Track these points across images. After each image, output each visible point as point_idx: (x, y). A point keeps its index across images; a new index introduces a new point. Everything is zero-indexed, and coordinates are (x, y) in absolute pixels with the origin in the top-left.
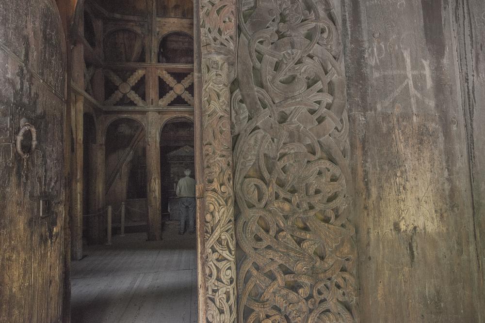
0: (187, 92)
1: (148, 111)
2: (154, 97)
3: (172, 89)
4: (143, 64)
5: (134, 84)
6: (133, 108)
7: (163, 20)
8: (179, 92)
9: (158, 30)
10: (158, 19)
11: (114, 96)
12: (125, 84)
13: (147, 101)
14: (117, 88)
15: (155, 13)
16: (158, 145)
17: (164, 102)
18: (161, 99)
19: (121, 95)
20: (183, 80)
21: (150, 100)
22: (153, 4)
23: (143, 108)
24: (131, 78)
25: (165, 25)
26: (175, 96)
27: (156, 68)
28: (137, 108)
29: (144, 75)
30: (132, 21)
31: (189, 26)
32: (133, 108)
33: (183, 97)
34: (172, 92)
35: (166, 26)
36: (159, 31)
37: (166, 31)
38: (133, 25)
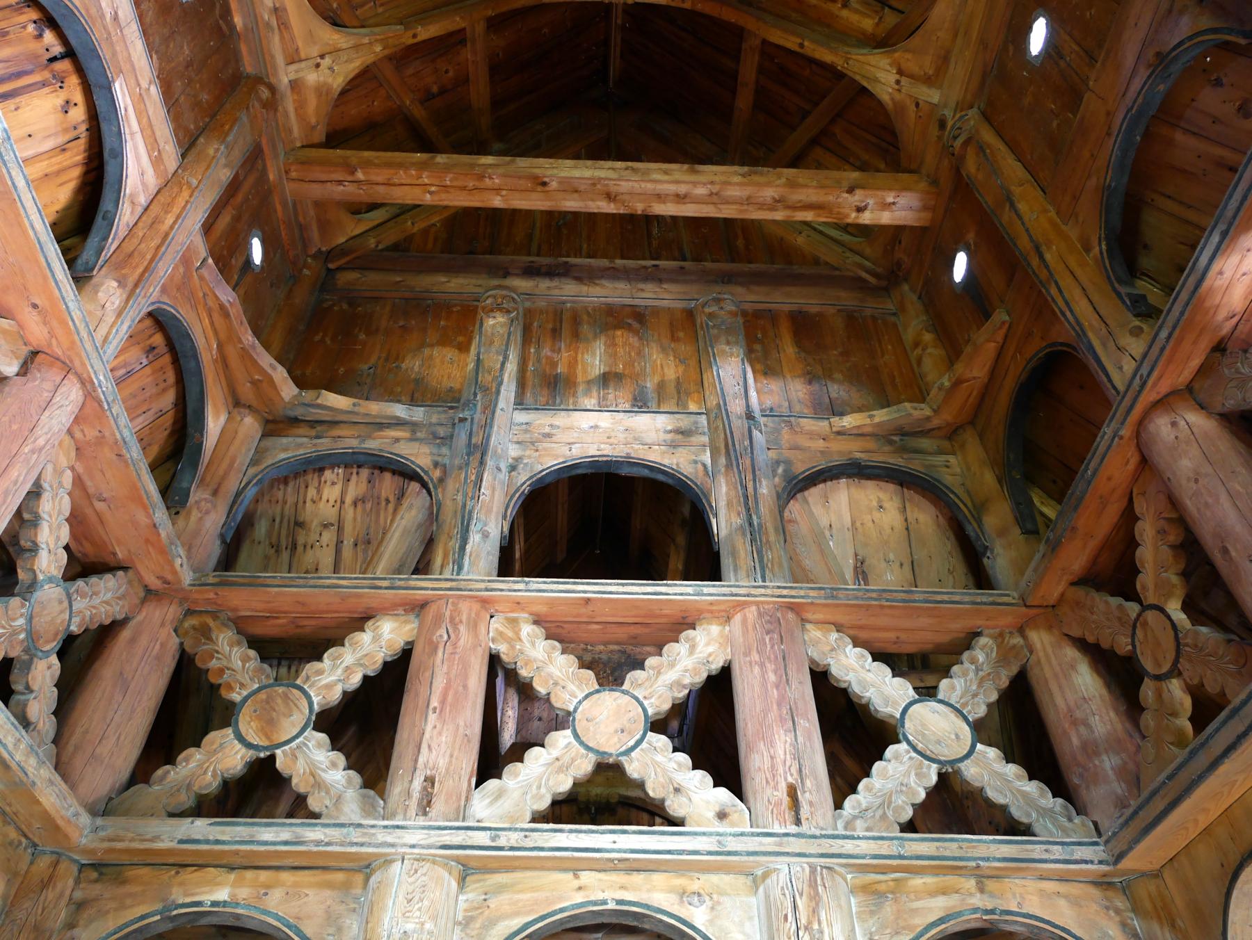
0: (661, 741)
1: (388, 862)
2: (442, 763)
3: (561, 721)
4: (418, 581)
5: (335, 696)
6: (285, 835)
7: (542, 421)
8: (612, 746)
9: (513, 451)
10: (521, 417)
12: (281, 690)
13: (396, 789)
14: (225, 714)
15: (508, 391)
17: (506, 805)
18: (492, 784)
20: (637, 674)
21: (418, 784)
22: (503, 364)
23: (355, 835)
25: (549, 435)
26: (585, 766)
27: (485, 602)
28: (313, 834)
29: (406, 654)
30: (399, 423)
31: (669, 437)
32: (285, 835)
33: (633, 769)
35: (554, 439)
36: (518, 460)
37: (557, 457)
38: (397, 440)
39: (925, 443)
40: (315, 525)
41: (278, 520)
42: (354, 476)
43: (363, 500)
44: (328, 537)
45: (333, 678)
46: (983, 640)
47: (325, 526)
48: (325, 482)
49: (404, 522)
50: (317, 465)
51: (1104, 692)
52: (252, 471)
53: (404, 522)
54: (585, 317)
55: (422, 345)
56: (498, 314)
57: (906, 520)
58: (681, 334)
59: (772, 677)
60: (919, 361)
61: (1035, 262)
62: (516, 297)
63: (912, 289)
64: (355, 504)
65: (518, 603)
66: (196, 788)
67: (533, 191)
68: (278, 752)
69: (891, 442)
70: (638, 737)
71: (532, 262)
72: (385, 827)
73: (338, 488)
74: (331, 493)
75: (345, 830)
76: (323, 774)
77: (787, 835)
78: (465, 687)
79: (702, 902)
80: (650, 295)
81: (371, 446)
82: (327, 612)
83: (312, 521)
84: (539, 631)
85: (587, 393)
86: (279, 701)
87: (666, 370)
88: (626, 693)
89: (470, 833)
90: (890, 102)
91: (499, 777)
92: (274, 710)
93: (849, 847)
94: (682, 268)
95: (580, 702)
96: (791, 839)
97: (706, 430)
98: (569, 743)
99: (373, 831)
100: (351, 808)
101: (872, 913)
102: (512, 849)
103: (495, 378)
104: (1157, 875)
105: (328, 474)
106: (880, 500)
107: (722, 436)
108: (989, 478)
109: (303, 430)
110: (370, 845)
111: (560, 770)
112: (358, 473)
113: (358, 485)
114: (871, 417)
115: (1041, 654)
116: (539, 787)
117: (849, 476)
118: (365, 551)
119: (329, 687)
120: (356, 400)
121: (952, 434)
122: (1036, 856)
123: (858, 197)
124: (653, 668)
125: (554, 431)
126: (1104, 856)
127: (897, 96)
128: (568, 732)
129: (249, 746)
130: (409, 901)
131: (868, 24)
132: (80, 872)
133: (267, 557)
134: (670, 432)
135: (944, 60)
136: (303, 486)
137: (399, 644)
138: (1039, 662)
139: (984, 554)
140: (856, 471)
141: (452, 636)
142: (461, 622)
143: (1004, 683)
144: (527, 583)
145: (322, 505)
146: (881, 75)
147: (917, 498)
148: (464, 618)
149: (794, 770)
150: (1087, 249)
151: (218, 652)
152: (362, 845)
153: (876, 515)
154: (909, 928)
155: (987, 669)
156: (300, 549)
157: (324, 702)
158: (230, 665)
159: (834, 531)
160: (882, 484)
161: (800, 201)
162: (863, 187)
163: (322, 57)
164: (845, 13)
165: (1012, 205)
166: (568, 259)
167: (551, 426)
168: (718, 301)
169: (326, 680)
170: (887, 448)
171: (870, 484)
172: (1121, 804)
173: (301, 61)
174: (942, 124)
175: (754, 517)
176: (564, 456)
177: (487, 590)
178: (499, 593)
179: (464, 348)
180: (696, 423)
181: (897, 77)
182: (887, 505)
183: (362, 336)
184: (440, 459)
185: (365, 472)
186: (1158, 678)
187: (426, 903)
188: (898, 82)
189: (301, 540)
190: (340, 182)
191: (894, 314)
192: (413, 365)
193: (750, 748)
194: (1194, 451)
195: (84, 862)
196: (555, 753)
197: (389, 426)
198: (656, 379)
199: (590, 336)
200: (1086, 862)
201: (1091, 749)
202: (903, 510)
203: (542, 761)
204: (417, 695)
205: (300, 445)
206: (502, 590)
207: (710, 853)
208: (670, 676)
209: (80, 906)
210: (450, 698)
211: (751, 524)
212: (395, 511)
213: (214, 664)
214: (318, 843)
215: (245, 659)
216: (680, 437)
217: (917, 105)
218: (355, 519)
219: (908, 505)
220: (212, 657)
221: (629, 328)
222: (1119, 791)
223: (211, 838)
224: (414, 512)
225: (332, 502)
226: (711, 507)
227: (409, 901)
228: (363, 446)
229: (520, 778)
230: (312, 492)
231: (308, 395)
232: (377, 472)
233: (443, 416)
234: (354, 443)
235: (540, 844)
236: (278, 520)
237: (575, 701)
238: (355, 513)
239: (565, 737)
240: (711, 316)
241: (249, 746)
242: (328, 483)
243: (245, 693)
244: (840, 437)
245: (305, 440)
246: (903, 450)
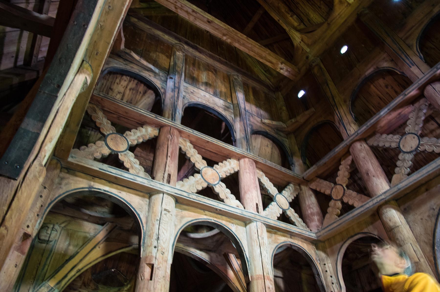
0: (224, 185)
11: (92, 147)
19: (106, 152)
21: (166, 176)
24: (132, 133)
34: (198, 176)
39: (282, 134)
40: (116, 91)
41: (104, 84)
43: (133, 89)
46: (291, 185)
47: (119, 93)
49: (145, 101)
50: (123, 73)
51: (317, 203)
52: (106, 66)
53: (145, 101)
54: (201, 64)
55: (156, 51)
56: (181, 52)
57: (272, 152)
58: (226, 80)
59: (252, 177)
60: (281, 114)
61: (331, 100)
63: (282, 94)
65: (189, 136)
66: (95, 156)
68: (119, 154)
69: (274, 130)
72: (159, 183)
74: (124, 83)
77: (256, 214)
78: (176, 153)
79: (234, 226)
80: (218, 65)
84: (192, 146)
85: (202, 85)
86: (119, 139)
87: (222, 88)
88: (214, 169)
90: (296, 46)
92: (117, 141)
93: (269, 221)
94: (226, 62)
96: (257, 216)
99: (156, 183)
101: (270, 237)
102: (193, 199)
103: (180, 70)
104: (324, 242)
105: (124, 77)
106: (268, 144)
107: (238, 112)
108: (296, 148)
109: (121, 60)
110: (155, 187)
111: (198, 184)
113: (133, 84)
114: (272, 122)
115: (304, 191)
116: (193, 187)
117: (263, 135)
119: (134, 140)
121: (288, 134)
122: (304, 233)
123: (282, 66)
125: (194, 92)
126: (315, 236)
127: (299, 45)
129: (110, 149)
131: (296, 24)
132: (61, 169)
134: (224, 105)
135: (315, 43)
136: (115, 77)
137: (153, 136)
138: (303, 193)
139: (291, 165)
140: (265, 135)
141: (173, 138)
143: (295, 196)
145: (120, 86)
146: (297, 38)
147: (276, 147)
148: (175, 135)
149: (258, 200)
150: (345, 102)
153: (266, 148)
154: (278, 242)
155: (292, 191)
157: (132, 144)
159: (255, 148)
160: (270, 140)
161: (269, 60)
162: (284, 63)
164: (291, 18)
165: (328, 85)
167: (193, 91)
168: (238, 76)
170: (273, 131)
171: (267, 139)
172: (318, 227)
174: (307, 58)
175: (247, 136)
176: (197, 100)
177: (182, 129)
178: (186, 131)
180: (230, 106)
181: (301, 41)
182: (269, 146)
183: (138, 40)
184: (163, 87)
186: (336, 200)
188: (300, 42)
191: (275, 99)
193: (245, 193)
194: (365, 152)
195: (63, 166)
196: (197, 179)
197: (148, 71)
198: (220, 90)
199: (203, 70)
200: (312, 236)
201: (312, 214)
202: (272, 149)
204: (163, 150)
205: (121, 65)
206: (186, 130)
207: (240, 214)
208: (225, 169)
209: (62, 179)
210: (173, 155)
211: (246, 138)
212: (142, 97)
213: (97, 121)
214: (141, 182)
215: (107, 123)
216: (226, 108)
217: (303, 50)
218: (129, 94)
219: (273, 148)
221: (212, 72)
222: (318, 224)
223: (109, 171)
224: (149, 99)
225: (123, 86)
226: (234, 129)
230: (118, 81)
231: (128, 51)
232: (139, 83)
234: (138, 71)
235: (200, 200)
236: (104, 84)
240: (235, 79)
241: (110, 149)
242: (124, 80)
243: (108, 133)
244: (263, 124)
245: (122, 64)
246: (277, 133)
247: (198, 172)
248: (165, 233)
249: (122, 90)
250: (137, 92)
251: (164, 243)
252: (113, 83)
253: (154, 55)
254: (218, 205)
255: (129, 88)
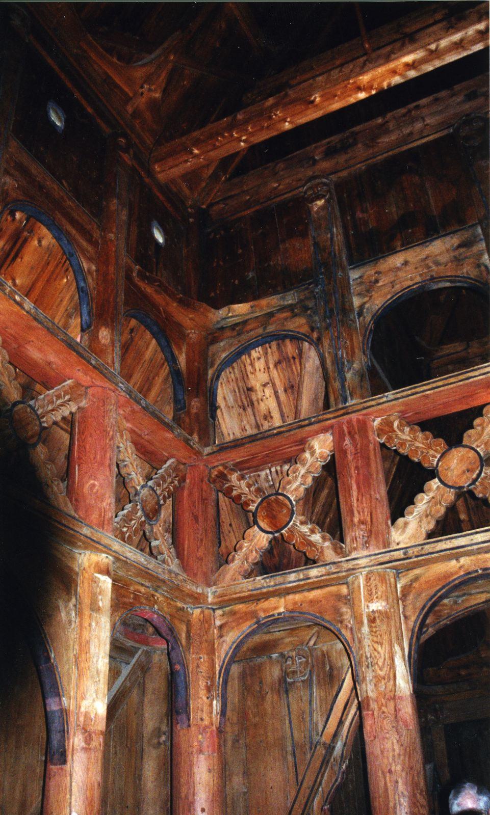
16: (407, 710)
18: (401, 521)
34: (435, 483)
40: (258, 387)
42: (269, 350)
43: (279, 362)
44: (268, 391)
45: (298, 483)
47: (265, 385)
48: (254, 359)
62: (324, 180)
64: (276, 366)
67: (307, 109)
70: (477, 472)
71: (329, 143)
72: (347, 561)
73: (262, 360)
74: (260, 365)
75: (327, 567)
76: (309, 538)
81: (271, 330)
82: (282, 446)
83: (256, 385)
89: (392, 553)
91: (403, 516)
92: (273, 510)
95: (439, 461)
97: (482, 237)
98: (438, 486)
100: (330, 555)
112: (270, 347)
118: (293, 393)
119: (296, 489)
120: (251, 303)
124: (479, 425)
128: (437, 480)
129: (267, 532)
130: (370, 595)
133: (239, 414)
142: (356, 433)
144: (387, 396)
145: (258, 373)
151: (234, 486)
152: (338, 572)
156: (256, 403)
158: (242, 492)
163: (142, 87)
166: (355, 129)
169: (294, 486)
173: (131, 99)
179: (304, 234)
185: (274, 344)
187: (379, 593)
189: (254, 398)
190: (186, 161)
192: (278, 261)
196: (431, 494)
203: (425, 501)
220: (232, 490)
225: (262, 370)
227: (370, 595)
228: (266, 331)
229: (415, 514)
233: (306, 292)
235: (431, 550)
237: (436, 460)
238: (278, 373)
239: (435, 484)
242: (256, 359)
243: (256, 505)
247: (432, 474)
248: (379, 649)
249: (263, 377)
250: (289, 361)
251: (381, 670)
252: (245, 377)
253: (278, 261)
254: (472, 540)
255: (271, 366)
